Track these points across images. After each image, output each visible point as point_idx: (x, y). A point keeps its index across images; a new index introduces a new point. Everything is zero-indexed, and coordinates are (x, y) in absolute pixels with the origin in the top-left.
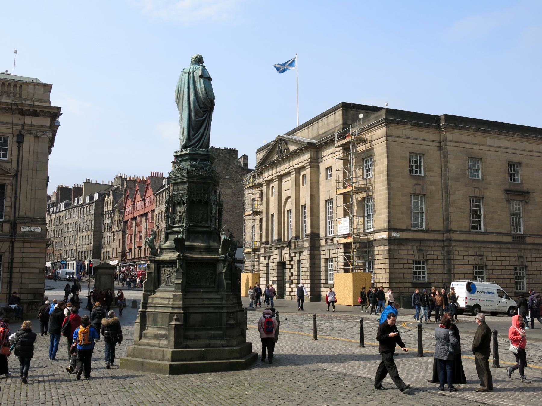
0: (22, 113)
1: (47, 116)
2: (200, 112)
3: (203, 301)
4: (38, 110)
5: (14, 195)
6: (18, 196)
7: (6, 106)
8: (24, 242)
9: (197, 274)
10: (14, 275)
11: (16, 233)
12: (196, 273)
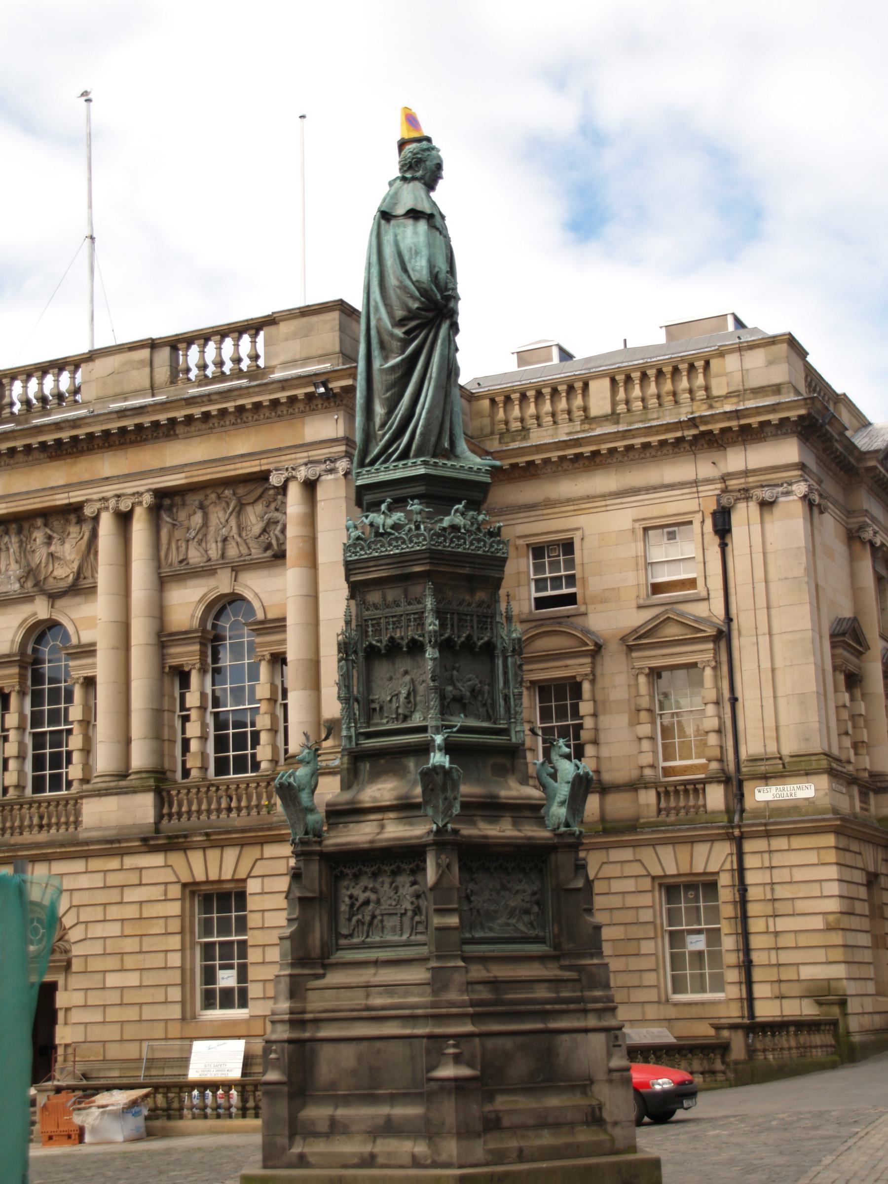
1: (786, 434)
3: (368, 996)
5: (726, 694)
8: (768, 835)
9: (367, 902)
10: (756, 942)
12: (362, 897)
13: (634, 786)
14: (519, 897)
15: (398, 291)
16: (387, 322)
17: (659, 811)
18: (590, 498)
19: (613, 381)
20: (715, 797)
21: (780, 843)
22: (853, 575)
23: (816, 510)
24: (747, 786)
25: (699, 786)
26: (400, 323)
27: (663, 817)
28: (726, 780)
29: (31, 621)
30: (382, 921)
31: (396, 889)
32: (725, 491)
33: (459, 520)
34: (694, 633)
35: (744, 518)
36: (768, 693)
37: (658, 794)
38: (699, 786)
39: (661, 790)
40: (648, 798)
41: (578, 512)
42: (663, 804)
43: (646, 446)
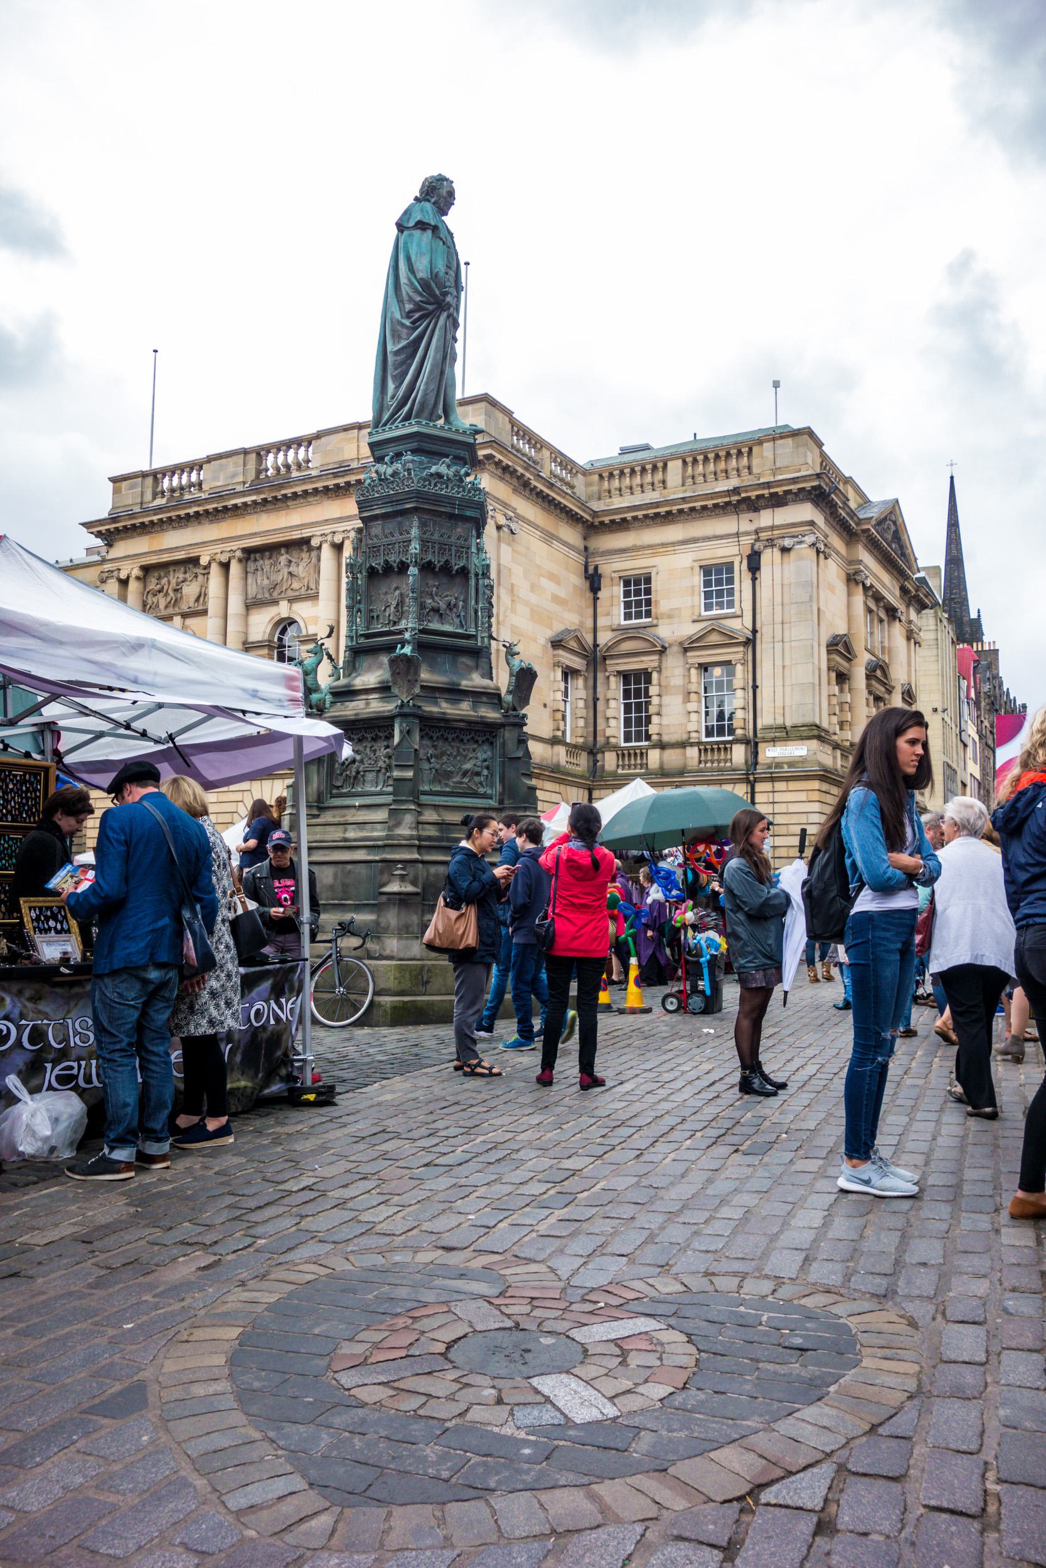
0: (753, 505)
1: (802, 500)
2: (403, 325)
3: (346, 830)
4: (779, 490)
5: (751, 684)
6: (758, 683)
7: (719, 501)
8: (772, 779)
11: (756, 763)
13: (683, 745)
14: (473, 762)
15: (408, 288)
16: (398, 316)
17: (700, 762)
18: (663, 545)
19: (685, 462)
20: (739, 754)
21: (779, 786)
22: (849, 606)
23: (822, 556)
24: (761, 746)
25: (728, 746)
26: (408, 315)
27: (702, 765)
28: (746, 741)
29: (276, 619)
30: (363, 776)
31: (375, 751)
32: (758, 540)
33: (443, 469)
34: (730, 640)
35: (770, 558)
36: (779, 683)
37: (700, 750)
38: (728, 746)
39: (702, 747)
40: (692, 753)
41: (654, 555)
42: (703, 758)
43: (704, 508)
